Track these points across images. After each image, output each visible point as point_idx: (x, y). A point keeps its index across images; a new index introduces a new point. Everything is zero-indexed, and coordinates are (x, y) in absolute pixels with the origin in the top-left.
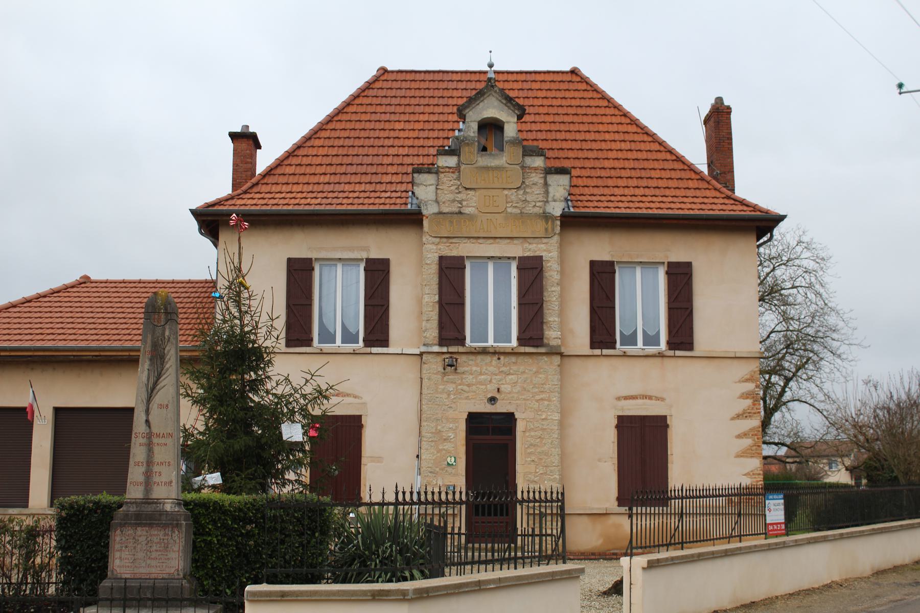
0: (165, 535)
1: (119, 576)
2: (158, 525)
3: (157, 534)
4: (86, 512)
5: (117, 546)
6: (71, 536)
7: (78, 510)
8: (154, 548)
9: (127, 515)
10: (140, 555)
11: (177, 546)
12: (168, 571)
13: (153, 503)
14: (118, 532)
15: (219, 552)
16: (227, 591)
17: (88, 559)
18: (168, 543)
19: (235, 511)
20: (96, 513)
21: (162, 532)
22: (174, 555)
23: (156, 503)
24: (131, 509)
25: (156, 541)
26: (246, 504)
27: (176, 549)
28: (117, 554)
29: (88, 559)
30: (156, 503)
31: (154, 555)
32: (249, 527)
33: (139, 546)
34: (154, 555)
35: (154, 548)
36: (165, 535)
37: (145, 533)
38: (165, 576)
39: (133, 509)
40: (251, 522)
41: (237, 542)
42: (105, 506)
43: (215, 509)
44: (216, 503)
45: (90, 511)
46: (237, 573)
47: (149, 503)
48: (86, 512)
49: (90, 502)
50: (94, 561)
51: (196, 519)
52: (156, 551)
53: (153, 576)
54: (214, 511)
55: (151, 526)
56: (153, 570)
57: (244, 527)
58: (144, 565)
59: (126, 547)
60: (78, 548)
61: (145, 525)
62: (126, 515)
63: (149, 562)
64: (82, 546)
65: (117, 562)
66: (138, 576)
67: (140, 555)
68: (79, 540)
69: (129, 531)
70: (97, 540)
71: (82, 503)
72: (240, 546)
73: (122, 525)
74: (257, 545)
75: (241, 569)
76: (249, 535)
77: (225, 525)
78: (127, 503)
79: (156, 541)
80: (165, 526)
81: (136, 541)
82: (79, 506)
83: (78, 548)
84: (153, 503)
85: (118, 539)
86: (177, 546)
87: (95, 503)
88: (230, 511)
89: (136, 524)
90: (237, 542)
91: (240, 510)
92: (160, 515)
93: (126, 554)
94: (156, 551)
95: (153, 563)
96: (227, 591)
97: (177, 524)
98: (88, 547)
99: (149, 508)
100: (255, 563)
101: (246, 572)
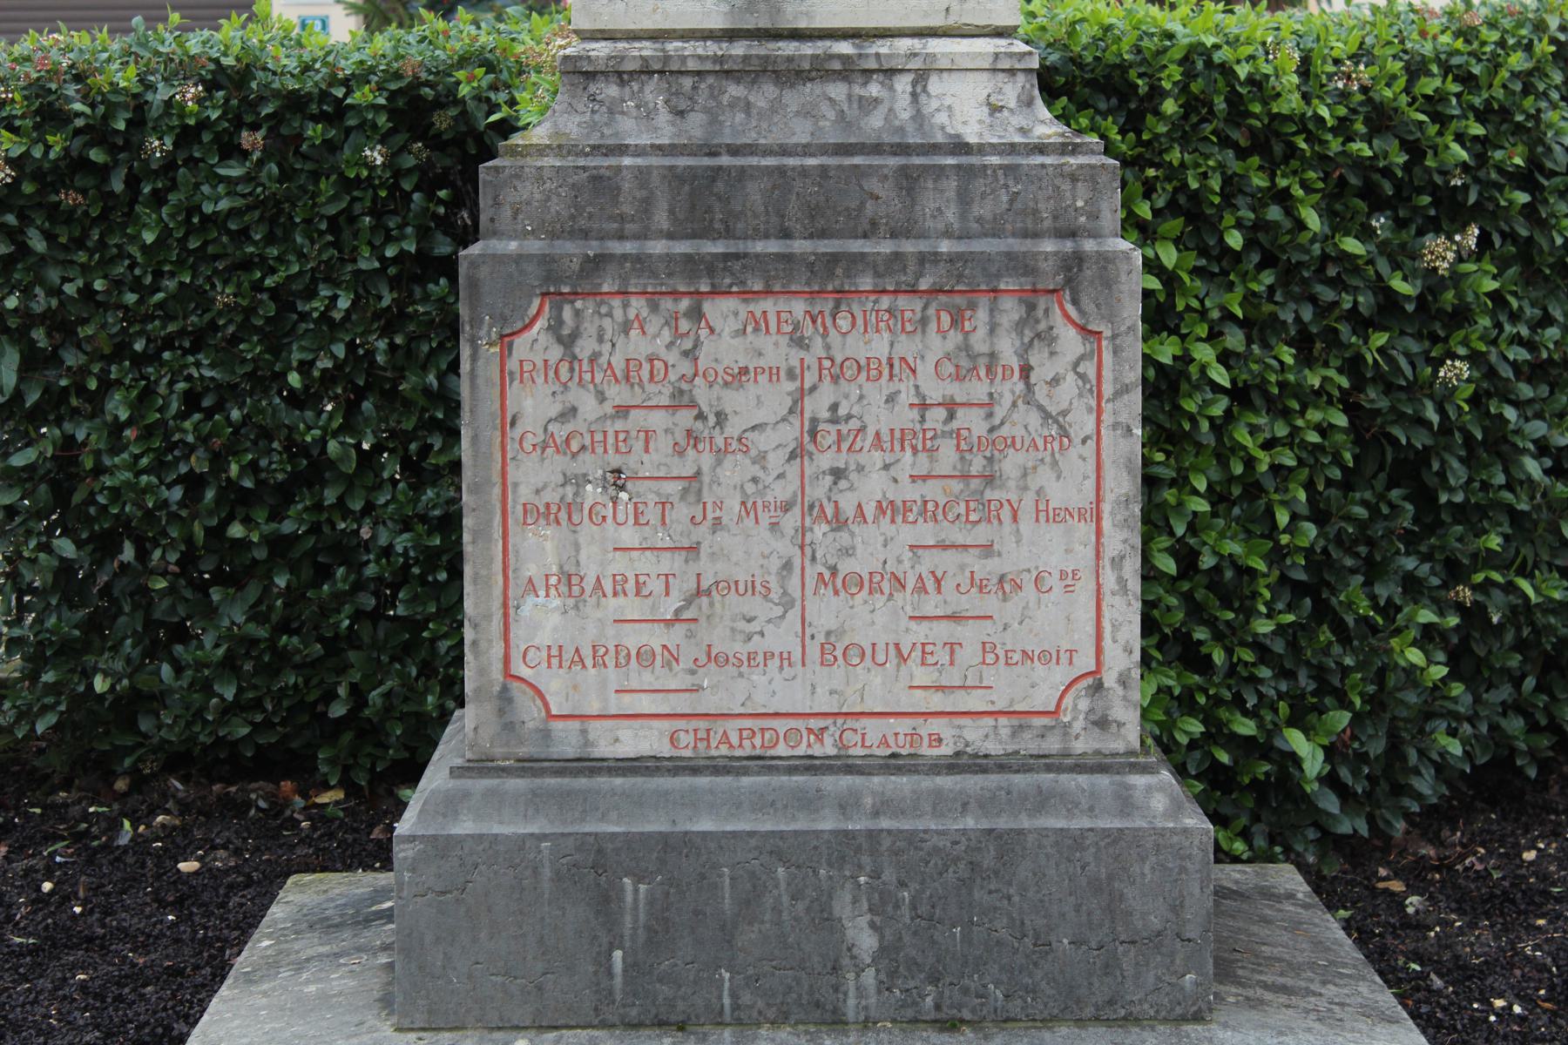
0: (968, 363)
1: (566, 742)
2: (895, 275)
3: (895, 359)
4: (158, 146)
5: (533, 476)
6: (62, 326)
7: (98, 133)
8: (872, 487)
9: (602, 184)
10: (749, 550)
11: (1078, 462)
12: (1005, 688)
13: (820, 71)
14: (535, 345)
15: (1224, 452)
16: (1296, 741)
17: (194, 483)
18: (995, 443)
19: (1343, 128)
20: (230, 150)
21: (938, 344)
22: (1056, 549)
23: (848, 71)
24: (631, 131)
25: (880, 418)
26: (1416, 69)
27: (1071, 490)
28: (539, 549)
29: (194, 483)
30: (848, 71)
31: (872, 547)
32: (1440, 252)
33: (735, 471)
34: (872, 547)
35: (872, 487)
36: (968, 363)
37: (775, 351)
38: (978, 737)
39: (647, 127)
40: (1450, 211)
41: (1354, 365)
42: (295, 103)
43: (1194, 105)
44: (1197, 59)
45: (187, 136)
46: (1355, 598)
47: (792, 75)
48: (158, 146)
49: (180, 69)
50: (237, 502)
51: (1173, 209)
52: (890, 509)
53: (873, 738)
54: (1184, 131)
55: (829, 279)
56: (875, 688)
57: (1401, 256)
58: (783, 638)
59: (617, 479)
60: (118, 407)
61: (779, 274)
62: (596, 190)
63: (826, 611)
64: (148, 393)
65: (543, 621)
66: (732, 740)
67: (749, 550)
68: (121, 350)
69: (634, 334)
70: (251, 349)
71: (126, 78)
72: (1373, 397)
73: (565, 284)
74: (1490, 386)
75: (1373, 571)
76: (1439, 316)
77: (1268, 248)
78: (580, 74)
79: (880, 418)
80: (960, 284)
81: (703, 426)
82: (107, 103)
83: (118, 407)
84: (820, 71)
85: (534, 405)
86: (1078, 462)
87: (218, 79)
88: (1310, 127)
89: (692, 265)
90: (1354, 365)
91: (1380, 119)
92: (909, 181)
93: (609, 544)
94: (890, 509)
95: (872, 620)
96: (1296, 741)
97: (1073, 264)
98: (191, 401)
99: (796, 122)
100: (1473, 516)
101: (1412, 586)
